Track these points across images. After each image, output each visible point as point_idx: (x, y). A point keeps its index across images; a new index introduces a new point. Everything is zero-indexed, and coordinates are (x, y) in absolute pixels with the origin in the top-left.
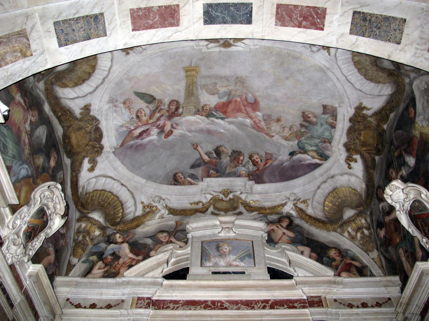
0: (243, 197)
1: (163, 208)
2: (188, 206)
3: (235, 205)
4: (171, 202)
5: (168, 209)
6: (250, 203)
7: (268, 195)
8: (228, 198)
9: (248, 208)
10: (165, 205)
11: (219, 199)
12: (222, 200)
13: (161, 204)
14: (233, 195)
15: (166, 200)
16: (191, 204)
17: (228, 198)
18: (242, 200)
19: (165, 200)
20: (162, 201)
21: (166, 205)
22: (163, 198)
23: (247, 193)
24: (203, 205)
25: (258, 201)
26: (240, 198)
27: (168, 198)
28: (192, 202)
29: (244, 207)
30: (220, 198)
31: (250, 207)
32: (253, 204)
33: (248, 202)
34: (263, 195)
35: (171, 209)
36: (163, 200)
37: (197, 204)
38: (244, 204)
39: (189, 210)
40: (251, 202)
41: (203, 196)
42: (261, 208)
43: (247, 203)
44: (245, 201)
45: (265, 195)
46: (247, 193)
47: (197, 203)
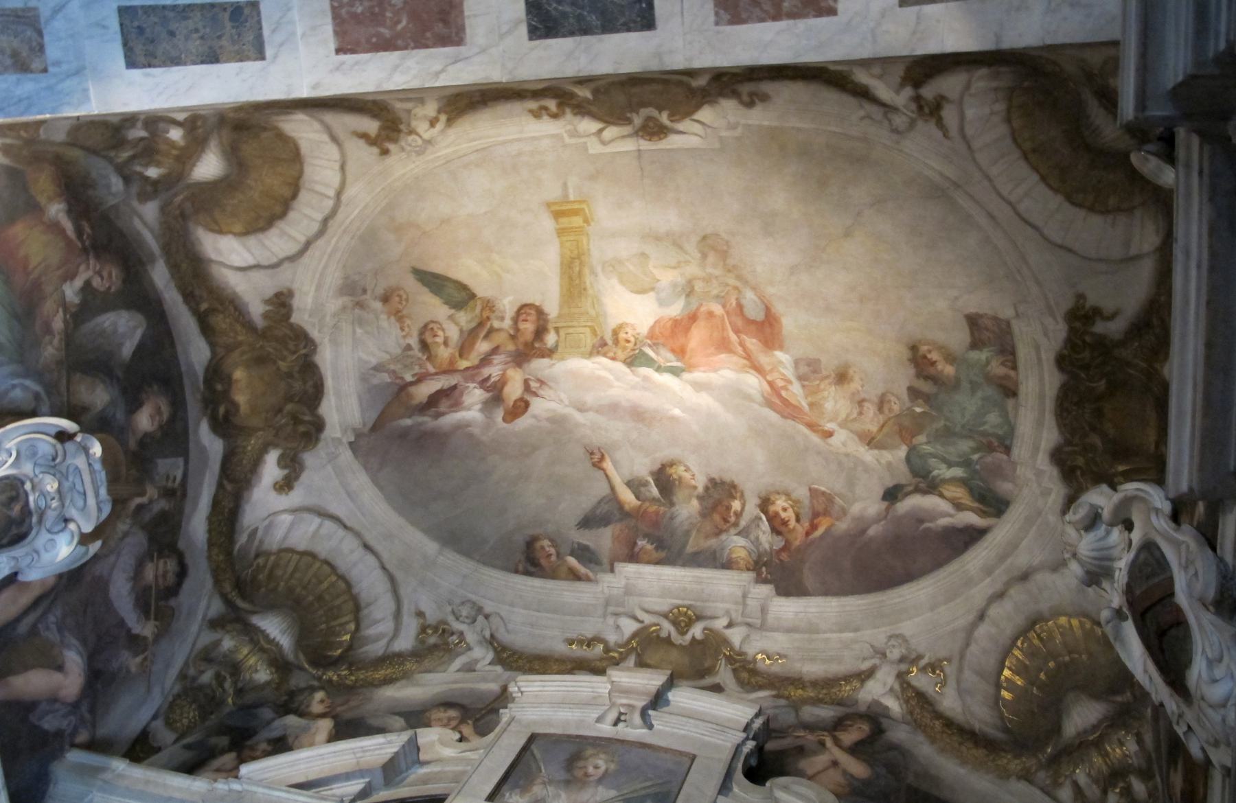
0: (736, 636)
1: (480, 643)
2: (561, 648)
3: (707, 664)
4: (510, 626)
5: (495, 649)
6: (755, 661)
7: (815, 636)
8: (688, 637)
9: (745, 675)
10: (488, 635)
11: (658, 636)
12: (668, 641)
13: (478, 629)
14: (705, 629)
15: (495, 620)
16: (571, 642)
17: (688, 637)
18: (732, 649)
19: (491, 619)
20: (480, 618)
21: (492, 636)
22: (487, 610)
23: (749, 625)
24: (607, 650)
25: (781, 656)
26: (726, 642)
27: (502, 614)
28: (574, 636)
29: (735, 671)
30: (664, 634)
31: (754, 672)
32: (764, 664)
33: (749, 658)
34: (797, 636)
35: (504, 648)
36: (487, 617)
37: (589, 646)
38: (736, 661)
39: (557, 660)
40: (759, 656)
41: (611, 620)
42: (787, 679)
43: (745, 660)
44: (741, 654)
45: (806, 636)
46: (749, 625)
47: (590, 643)
